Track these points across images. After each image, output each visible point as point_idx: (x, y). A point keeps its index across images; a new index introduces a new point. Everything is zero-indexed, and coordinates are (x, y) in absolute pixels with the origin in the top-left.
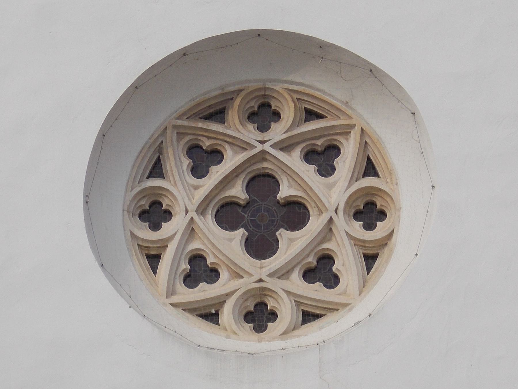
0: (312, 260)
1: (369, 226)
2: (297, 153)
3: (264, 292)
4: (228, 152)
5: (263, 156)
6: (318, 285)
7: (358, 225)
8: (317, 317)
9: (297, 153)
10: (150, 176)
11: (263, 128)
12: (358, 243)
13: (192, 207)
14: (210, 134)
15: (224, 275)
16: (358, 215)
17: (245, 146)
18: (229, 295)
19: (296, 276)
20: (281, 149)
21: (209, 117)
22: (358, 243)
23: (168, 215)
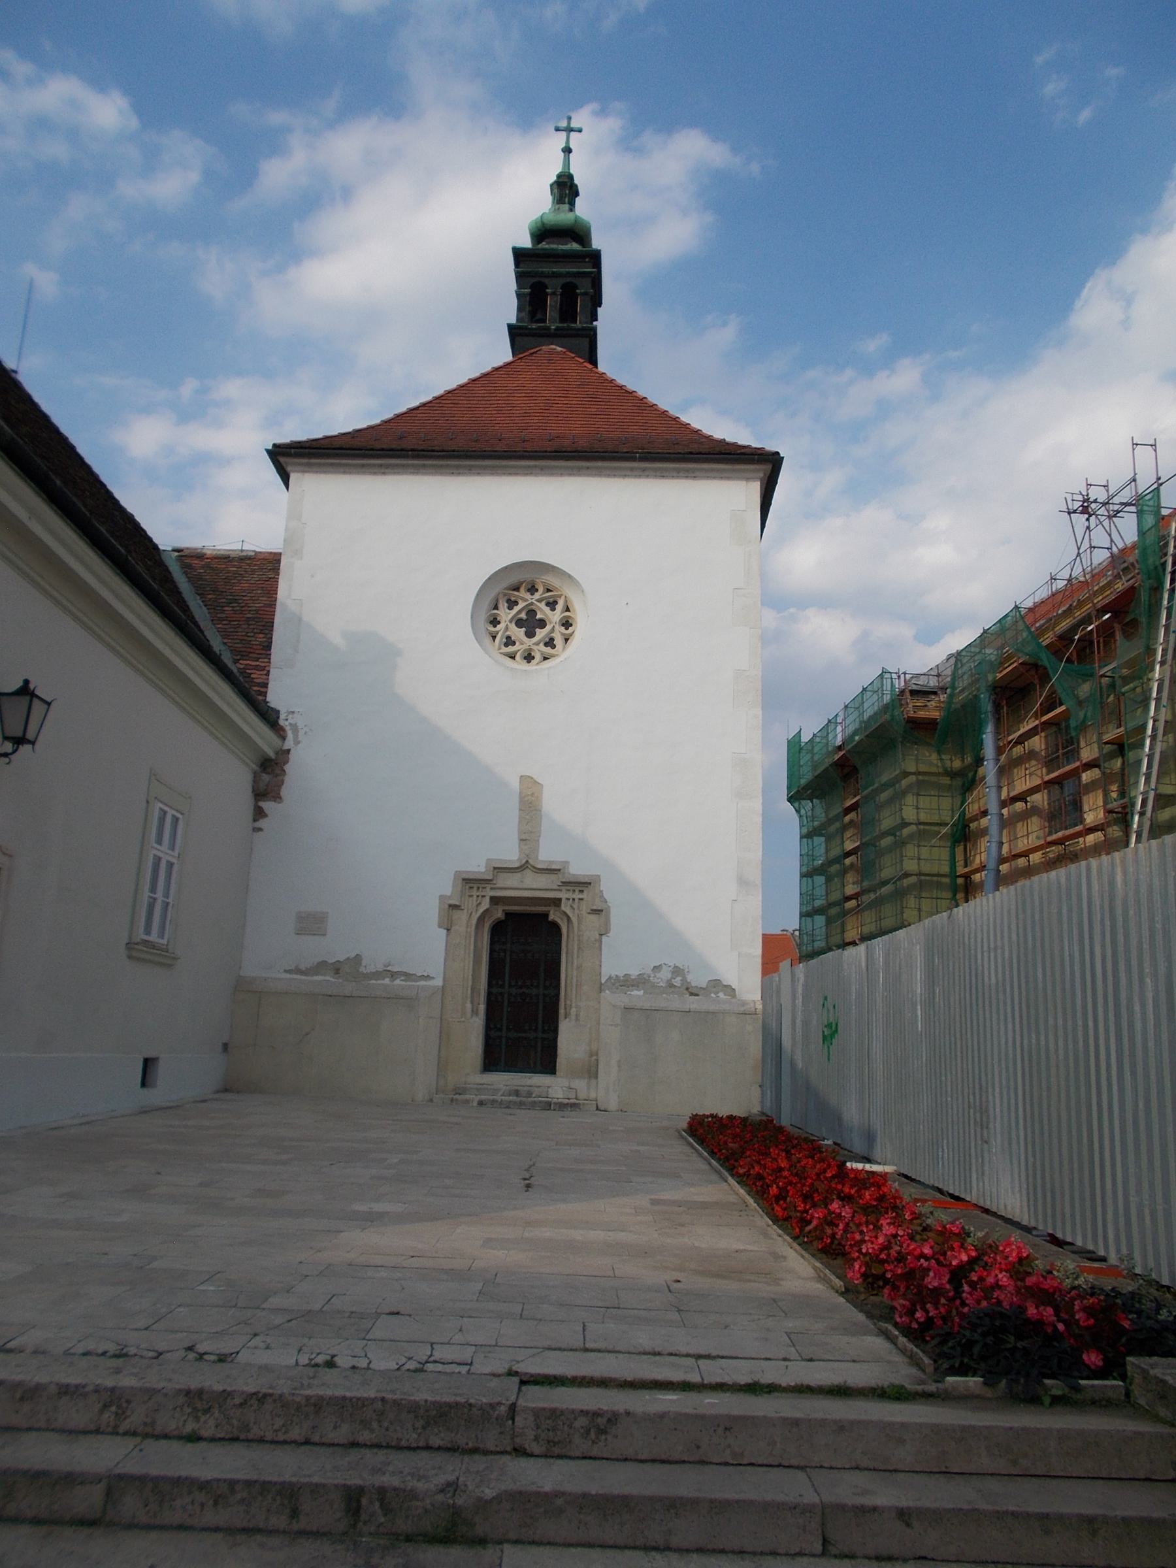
0: (547, 640)
1: (567, 629)
2: (543, 603)
3: (531, 650)
4: (520, 602)
5: (532, 604)
6: (549, 648)
7: (563, 628)
8: (548, 658)
9: (543, 603)
10: (494, 609)
11: (532, 594)
12: (563, 634)
14: (515, 596)
15: (517, 643)
16: (563, 625)
17: (526, 600)
19: (542, 645)
21: (514, 590)
22: (563, 634)
23: (499, 623)
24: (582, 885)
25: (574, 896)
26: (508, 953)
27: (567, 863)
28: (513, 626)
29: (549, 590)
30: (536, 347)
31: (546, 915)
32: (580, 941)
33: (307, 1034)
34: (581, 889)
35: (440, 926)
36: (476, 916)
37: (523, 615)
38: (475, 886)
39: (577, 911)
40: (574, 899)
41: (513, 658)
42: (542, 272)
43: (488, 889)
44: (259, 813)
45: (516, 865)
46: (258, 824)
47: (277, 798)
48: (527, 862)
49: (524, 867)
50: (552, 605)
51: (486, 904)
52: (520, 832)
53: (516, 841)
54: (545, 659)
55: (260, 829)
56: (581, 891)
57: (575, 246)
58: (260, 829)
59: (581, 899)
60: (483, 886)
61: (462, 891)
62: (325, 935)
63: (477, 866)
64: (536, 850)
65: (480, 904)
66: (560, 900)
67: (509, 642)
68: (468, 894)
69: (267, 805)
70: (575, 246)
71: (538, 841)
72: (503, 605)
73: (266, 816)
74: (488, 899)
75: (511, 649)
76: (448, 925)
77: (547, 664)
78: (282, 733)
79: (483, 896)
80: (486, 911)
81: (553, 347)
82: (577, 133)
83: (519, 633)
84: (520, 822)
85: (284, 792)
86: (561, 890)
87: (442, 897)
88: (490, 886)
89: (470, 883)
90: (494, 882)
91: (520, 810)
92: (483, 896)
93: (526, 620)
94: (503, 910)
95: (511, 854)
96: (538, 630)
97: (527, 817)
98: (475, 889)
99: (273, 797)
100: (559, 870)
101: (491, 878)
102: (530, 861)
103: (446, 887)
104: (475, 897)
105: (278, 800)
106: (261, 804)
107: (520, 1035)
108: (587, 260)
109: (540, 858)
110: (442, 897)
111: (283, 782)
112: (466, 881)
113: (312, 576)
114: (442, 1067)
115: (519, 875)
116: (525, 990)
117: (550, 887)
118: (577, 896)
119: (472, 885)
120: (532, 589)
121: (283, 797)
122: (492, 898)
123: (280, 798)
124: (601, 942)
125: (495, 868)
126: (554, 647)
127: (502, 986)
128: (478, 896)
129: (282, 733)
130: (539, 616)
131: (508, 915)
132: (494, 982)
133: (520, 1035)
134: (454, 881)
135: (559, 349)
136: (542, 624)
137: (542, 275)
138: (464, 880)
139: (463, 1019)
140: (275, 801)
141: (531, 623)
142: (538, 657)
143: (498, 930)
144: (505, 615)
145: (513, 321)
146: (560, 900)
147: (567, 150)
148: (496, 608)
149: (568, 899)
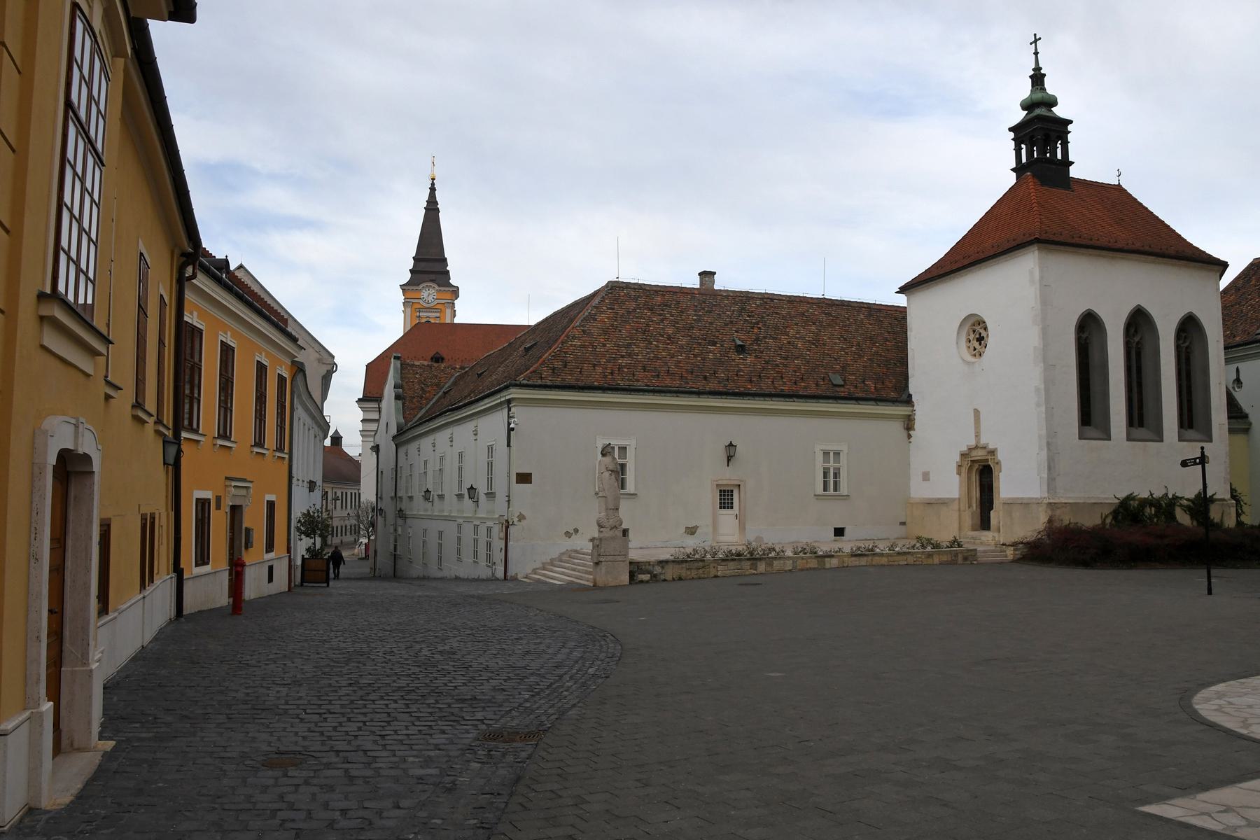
24: (993, 452)
27: (988, 444)
36: (967, 468)
37: (978, 336)
44: (909, 436)
47: (914, 430)
49: (977, 447)
64: (979, 439)
67: (975, 349)
69: (911, 432)
76: (959, 473)
80: (971, 466)
83: (976, 344)
89: (963, 455)
95: (973, 443)
103: (957, 458)
106: (910, 432)
109: (982, 443)
112: (962, 455)
131: (984, 466)
135: (1029, 173)
145: (1014, 165)
147: (1036, 53)
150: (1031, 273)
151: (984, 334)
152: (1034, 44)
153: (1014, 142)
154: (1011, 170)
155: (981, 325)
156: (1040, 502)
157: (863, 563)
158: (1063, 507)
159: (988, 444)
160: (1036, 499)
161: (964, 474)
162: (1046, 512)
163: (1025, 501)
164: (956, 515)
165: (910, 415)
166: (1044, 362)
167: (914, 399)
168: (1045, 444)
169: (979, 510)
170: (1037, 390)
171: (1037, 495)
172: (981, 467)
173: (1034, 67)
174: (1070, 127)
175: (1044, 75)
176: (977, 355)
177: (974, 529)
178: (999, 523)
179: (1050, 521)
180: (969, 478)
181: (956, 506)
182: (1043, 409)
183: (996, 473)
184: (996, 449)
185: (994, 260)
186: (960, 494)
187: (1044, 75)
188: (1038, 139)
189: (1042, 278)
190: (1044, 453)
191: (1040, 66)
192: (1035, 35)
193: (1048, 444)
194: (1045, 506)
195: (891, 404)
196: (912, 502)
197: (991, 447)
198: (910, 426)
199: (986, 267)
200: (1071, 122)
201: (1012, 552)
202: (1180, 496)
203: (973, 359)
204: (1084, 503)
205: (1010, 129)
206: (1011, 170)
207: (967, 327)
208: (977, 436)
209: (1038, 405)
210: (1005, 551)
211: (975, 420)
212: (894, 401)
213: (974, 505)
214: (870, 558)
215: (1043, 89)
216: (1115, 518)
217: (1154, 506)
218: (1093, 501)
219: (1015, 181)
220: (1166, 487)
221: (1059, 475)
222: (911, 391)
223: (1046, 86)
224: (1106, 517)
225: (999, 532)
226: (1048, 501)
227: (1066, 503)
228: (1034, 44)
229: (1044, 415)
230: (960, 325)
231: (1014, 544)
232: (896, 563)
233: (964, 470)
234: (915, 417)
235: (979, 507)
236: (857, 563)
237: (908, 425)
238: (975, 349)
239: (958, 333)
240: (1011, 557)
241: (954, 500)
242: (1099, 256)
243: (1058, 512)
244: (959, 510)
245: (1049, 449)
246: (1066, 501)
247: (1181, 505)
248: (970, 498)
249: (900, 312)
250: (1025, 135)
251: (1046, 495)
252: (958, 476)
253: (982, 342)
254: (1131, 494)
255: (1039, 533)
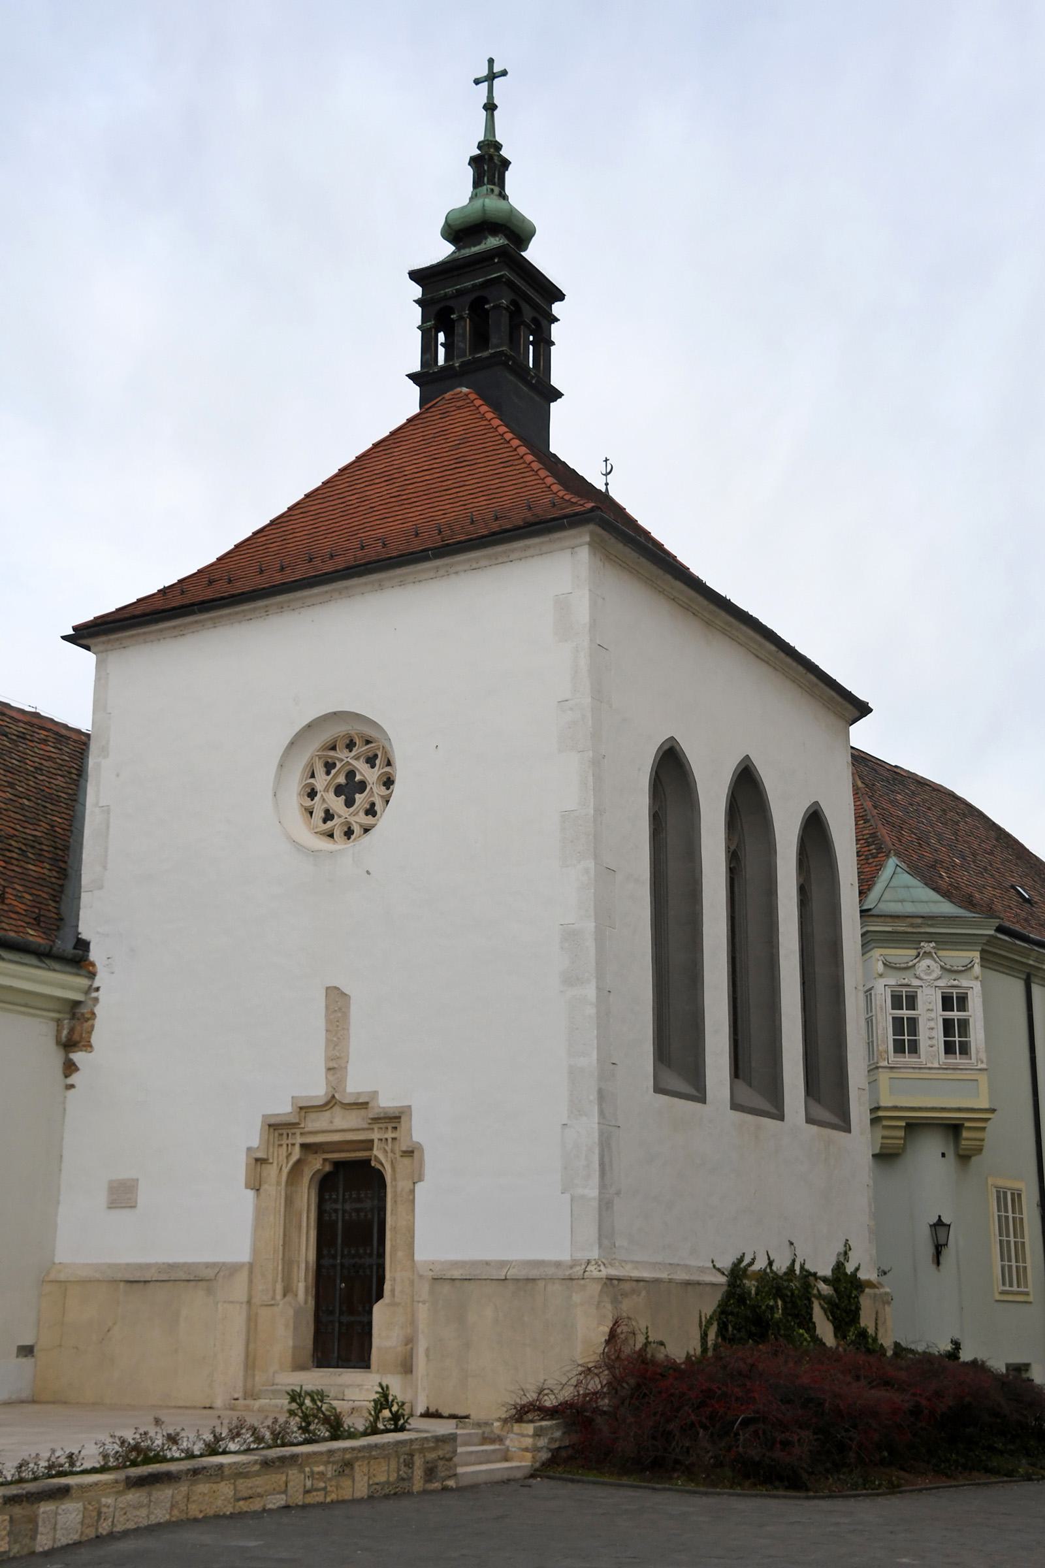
8: (369, 830)
12: (382, 797)
13: (322, 789)
14: (331, 757)
15: (336, 817)
17: (343, 760)
18: (335, 825)
20: (356, 759)
22: (382, 797)
24: (394, 1120)
25: (386, 1136)
26: (340, 1213)
27: (376, 1093)
28: (331, 796)
29: (368, 742)
30: (439, 396)
31: (367, 1162)
32: (395, 1192)
33: (108, 1331)
34: (394, 1125)
35: (247, 1187)
36: (285, 1171)
37: (341, 780)
38: (285, 1132)
39: (390, 1155)
40: (387, 1139)
41: (331, 836)
42: (446, 294)
43: (298, 1136)
44: (70, 1068)
45: (321, 1102)
46: (70, 1081)
47: (88, 1047)
48: (333, 1097)
49: (331, 1103)
50: (371, 761)
51: (296, 1154)
52: (329, 1059)
53: (324, 1070)
54: (366, 831)
55: (72, 1086)
56: (395, 1128)
57: (493, 242)
58: (72, 1086)
59: (394, 1139)
60: (293, 1131)
61: (268, 1140)
62: (135, 1207)
63: (283, 1108)
64: (342, 1081)
65: (290, 1154)
66: (372, 1141)
67: (328, 816)
68: (277, 1143)
69: (77, 1057)
70: (493, 242)
71: (346, 1068)
72: (320, 771)
73: (77, 1069)
74: (297, 1149)
75: (330, 824)
76: (255, 1184)
77: (367, 838)
78: (91, 968)
79: (293, 1145)
80: (298, 1162)
81: (459, 389)
82: (502, 78)
83: (337, 804)
84: (327, 1046)
85: (94, 1039)
86: (373, 1129)
87: (249, 1149)
88: (298, 1131)
89: (277, 1128)
90: (302, 1126)
91: (327, 1031)
92: (293, 1145)
93: (347, 784)
94: (325, 1160)
95: (318, 1090)
96: (357, 796)
97: (335, 1039)
98: (285, 1136)
99: (84, 1046)
100: (367, 1103)
101: (297, 1121)
102: (337, 1096)
103: (253, 1137)
104: (285, 1146)
105: (89, 1049)
107: (352, 1319)
108: (496, 261)
110: (249, 1149)
111: (93, 1026)
113: (118, 775)
114: (250, 1363)
115: (327, 1114)
116: (357, 1260)
117: (360, 1127)
118: (390, 1135)
119: (280, 1131)
120: (350, 745)
121: (93, 1045)
122: (304, 1146)
123: (91, 1046)
124: (413, 1191)
125: (301, 1108)
126: (374, 814)
127: (334, 1257)
128: (288, 1145)
129: (91, 968)
130: (358, 778)
131: (338, 1165)
132: (325, 1252)
133: (352, 1319)
134: (262, 1126)
135: (465, 390)
136: (362, 787)
137: (446, 297)
138: (270, 1126)
139: (273, 1302)
140: (86, 1051)
141: (350, 789)
142: (357, 830)
143: (326, 1184)
144: (321, 781)
145: (416, 367)
146: (372, 1141)
147: (490, 107)
148: (313, 776)
149: (379, 1139)
150: (562, 606)
151: (365, 772)
152: (485, 85)
153: (418, 310)
154: (410, 376)
155: (360, 749)
156: (578, 1271)
157: (161, 1515)
158: (633, 1291)
159: (376, 1093)
160: (558, 1264)
161: (274, 1188)
162: (598, 1306)
163: (513, 1273)
164: (238, 1320)
165: (77, 1004)
166: (596, 857)
167: (95, 955)
168: (593, 1096)
169: (311, 1303)
170: (570, 936)
171: (565, 1256)
172: (328, 1168)
173: (482, 138)
174: (557, 308)
175: (506, 164)
176: (338, 834)
177: (299, 1367)
178: (410, 1341)
179: (612, 1336)
180: (289, 1201)
181: (239, 1289)
182: (590, 991)
183: (403, 1185)
184: (410, 1107)
185: (438, 562)
186: (255, 1251)
187: (506, 164)
188: (497, 307)
189: (594, 624)
190: (588, 1127)
191: (498, 139)
192: (491, 61)
193: (602, 1096)
194: (595, 1289)
195: (34, 960)
196: (62, 1277)
197: (387, 1101)
198: (76, 1037)
199: (402, 584)
200: (560, 296)
201: (529, 1442)
202: (812, 1271)
203: (324, 844)
204: (670, 1281)
205: (416, 276)
206: (410, 376)
207: (312, 749)
208: (335, 1068)
209: (570, 980)
210: (500, 1439)
211: (329, 1021)
212: (44, 956)
213: (301, 1287)
214: (184, 1488)
215: (503, 196)
216: (722, 1331)
217: (783, 1299)
218: (682, 1276)
219: (417, 410)
220: (792, 1244)
221: (618, 1193)
222: (86, 930)
223: (508, 190)
224: (709, 1323)
225: (407, 1367)
226: (605, 1272)
227: (638, 1281)
228: (485, 85)
229: (591, 1011)
230: (292, 743)
231: (521, 1413)
232: (256, 1505)
233: (275, 1175)
234: (97, 1010)
235: (312, 1291)
236: (141, 1517)
237: (72, 1031)
238: (328, 816)
239: (281, 766)
240: (525, 1462)
241: (231, 1270)
242: (686, 608)
243: (626, 1306)
244: (249, 1302)
245: (601, 1113)
246: (636, 1274)
247: (820, 1296)
248: (288, 1264)
249: (11, 718)
250: (460, 293)
251: (594, 1254)
252: (250, 1194)
253: (359, 797)
254: (741, 1260)
255: (588, 1371)
